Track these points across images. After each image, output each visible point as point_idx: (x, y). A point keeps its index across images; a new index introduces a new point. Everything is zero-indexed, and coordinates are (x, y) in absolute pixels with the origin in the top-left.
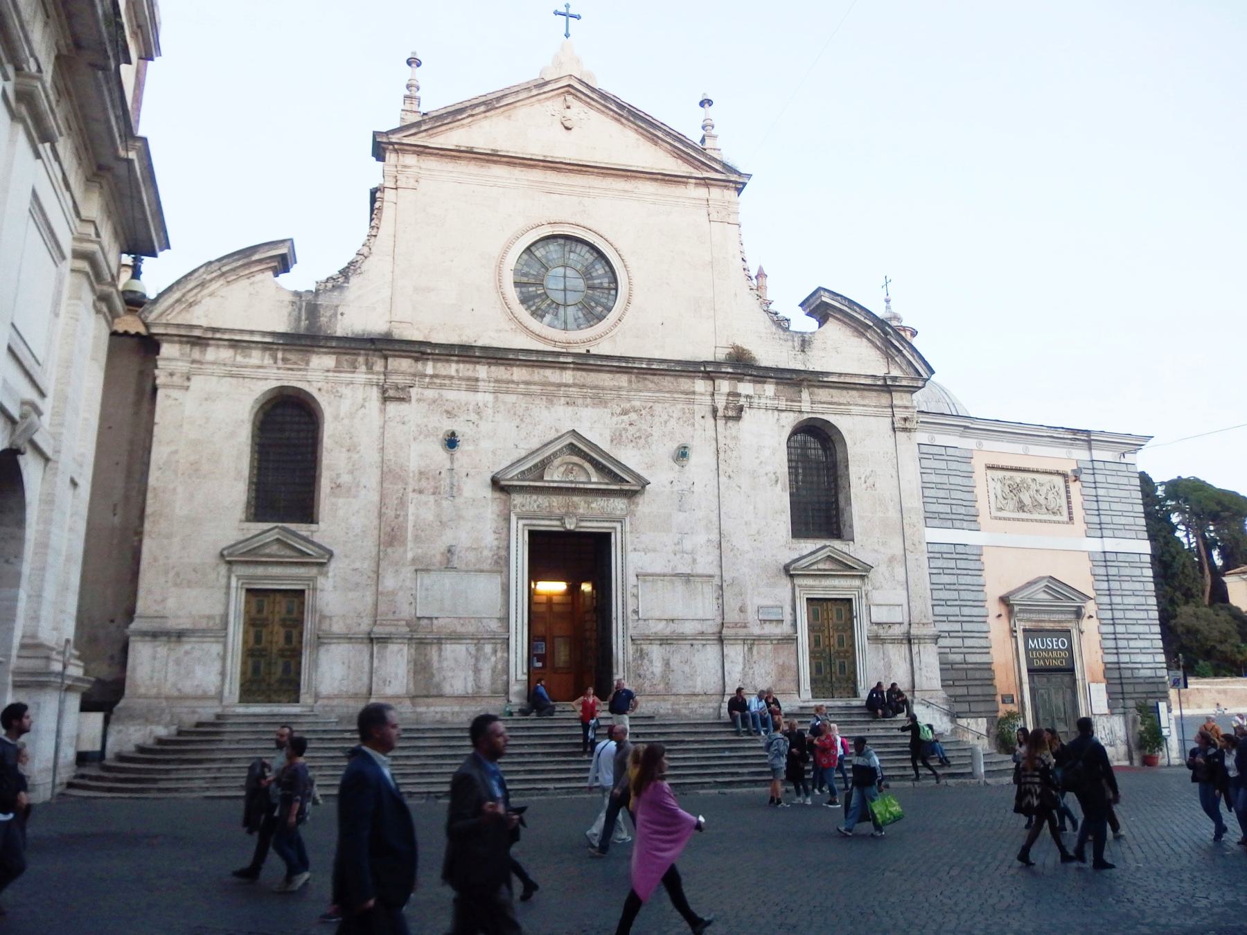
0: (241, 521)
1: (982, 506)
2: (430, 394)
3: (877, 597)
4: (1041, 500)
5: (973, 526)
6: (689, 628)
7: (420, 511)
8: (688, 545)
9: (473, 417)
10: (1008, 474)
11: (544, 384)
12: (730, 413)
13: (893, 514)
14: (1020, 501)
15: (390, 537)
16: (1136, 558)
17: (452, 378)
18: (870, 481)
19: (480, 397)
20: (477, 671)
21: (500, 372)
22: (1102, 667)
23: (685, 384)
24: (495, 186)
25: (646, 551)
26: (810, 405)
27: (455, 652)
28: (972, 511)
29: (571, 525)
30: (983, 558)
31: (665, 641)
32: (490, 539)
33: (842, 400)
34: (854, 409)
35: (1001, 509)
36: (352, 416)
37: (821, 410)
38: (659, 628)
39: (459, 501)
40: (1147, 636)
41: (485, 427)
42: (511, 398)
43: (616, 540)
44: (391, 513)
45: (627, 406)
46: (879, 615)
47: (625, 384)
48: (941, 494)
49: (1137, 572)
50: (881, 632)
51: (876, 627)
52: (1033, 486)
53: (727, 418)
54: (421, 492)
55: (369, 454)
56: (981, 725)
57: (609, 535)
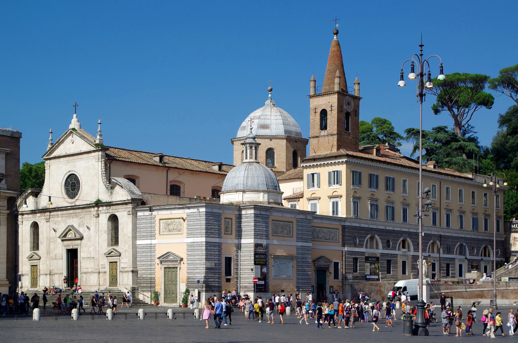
0: (30, 251)
1: (157, 232)
2: (53, 219)
3: (122, 261)
4: (175, 227)
5: (153, 238)
6: (90, 270)
7: (52, 247)
8: (90, 251)
9: (59, 224)
10: (167, 220)
11: (68, 214)
12: (97, 216)
13: (126, 238)
14: (169, 229)
15: (48, 253)
16: (200, 243)
17: (55, 215)
18: (122, 230)
19: (60, 219)
20: (59, 281)
21: (62, 212)
22: (187, 278)
23: (90, 209)
24: (61, 164)
25: (83, 252)
26: (112, 210)
27: (56, 276)
28: (153, 234)
29: (71, 248)
30: (156, 247)
31: (86, 273)
32: (61, 252)
33: (117, 208)
34: (120, 210)
35: (163, 232)
36: (42, 226)
37: (114, 212)
38: (85, 270)
39: (57, 243)
40: (200, 269)
41: (60, 225)
42: (64, 218)
43: (79, 250)
44: (47, 247)
45: (81, 217)
46: (122, 265)
47: (80, 211)
48: (145, 230)
49: (200, 248)
50: (123, 270)
51: (122, 269)
52: (174, 223)
53: (96, 217)
54: (52, 242)
55: (45, 235)
56: (149, 294)
57: (77, 249)
